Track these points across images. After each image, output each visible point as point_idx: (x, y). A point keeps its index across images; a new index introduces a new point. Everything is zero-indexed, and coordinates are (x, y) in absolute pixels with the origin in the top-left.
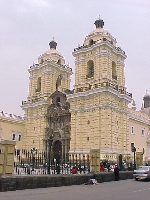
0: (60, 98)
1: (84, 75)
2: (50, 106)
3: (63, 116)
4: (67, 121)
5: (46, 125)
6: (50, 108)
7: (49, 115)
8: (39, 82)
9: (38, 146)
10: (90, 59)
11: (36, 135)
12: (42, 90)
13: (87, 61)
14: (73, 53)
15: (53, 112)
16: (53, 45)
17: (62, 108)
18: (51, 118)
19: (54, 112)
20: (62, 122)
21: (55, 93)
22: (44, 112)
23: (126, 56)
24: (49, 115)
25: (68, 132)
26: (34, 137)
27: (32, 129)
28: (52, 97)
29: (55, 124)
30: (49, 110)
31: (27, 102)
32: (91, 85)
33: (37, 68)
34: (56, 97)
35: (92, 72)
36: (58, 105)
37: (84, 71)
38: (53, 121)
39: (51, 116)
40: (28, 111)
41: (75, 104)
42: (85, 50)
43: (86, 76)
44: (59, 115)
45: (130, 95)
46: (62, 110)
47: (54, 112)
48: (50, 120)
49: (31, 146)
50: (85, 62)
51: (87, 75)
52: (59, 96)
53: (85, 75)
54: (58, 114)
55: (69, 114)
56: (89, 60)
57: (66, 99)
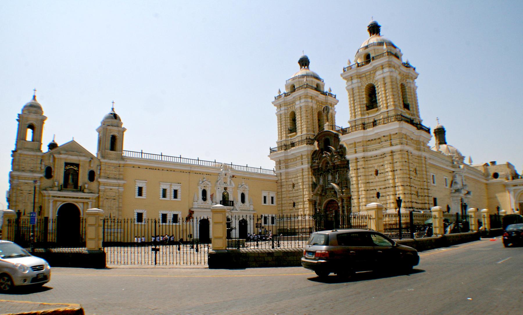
1: (362, 106)
2: (315, 152)
4: (344, 172)
5: (311, 179)
6: (315, 155)
8: (291, 119)
10: (369, 83)
11: (297, 194)
12: (299, 131)
13: (366, 85)
14: (342, 75)
16: (304, 62)
18: (318, 169)
20: (335, 174)
21: (318, 134)
23: (418, 74)
25: (347, 187)
27: (290, 186)
28: (317, 138)
29: (325, 176)
31: (276, 149)
32: (376, 119)
34: (323, 138)
35: (374, 100)
36: (329, 150)
37: (362, 100)
39: (318, 166)
40: (282, 162)
43: (367, 107)
44: (331, 165)
45: (427, 130)
48: (316, 171)
49: (291, 210)
50: (362, 87)
51: (367, 105)
52: (328, 137)
53: (365, 106)
54: (330, 162)
56: (367, 84)
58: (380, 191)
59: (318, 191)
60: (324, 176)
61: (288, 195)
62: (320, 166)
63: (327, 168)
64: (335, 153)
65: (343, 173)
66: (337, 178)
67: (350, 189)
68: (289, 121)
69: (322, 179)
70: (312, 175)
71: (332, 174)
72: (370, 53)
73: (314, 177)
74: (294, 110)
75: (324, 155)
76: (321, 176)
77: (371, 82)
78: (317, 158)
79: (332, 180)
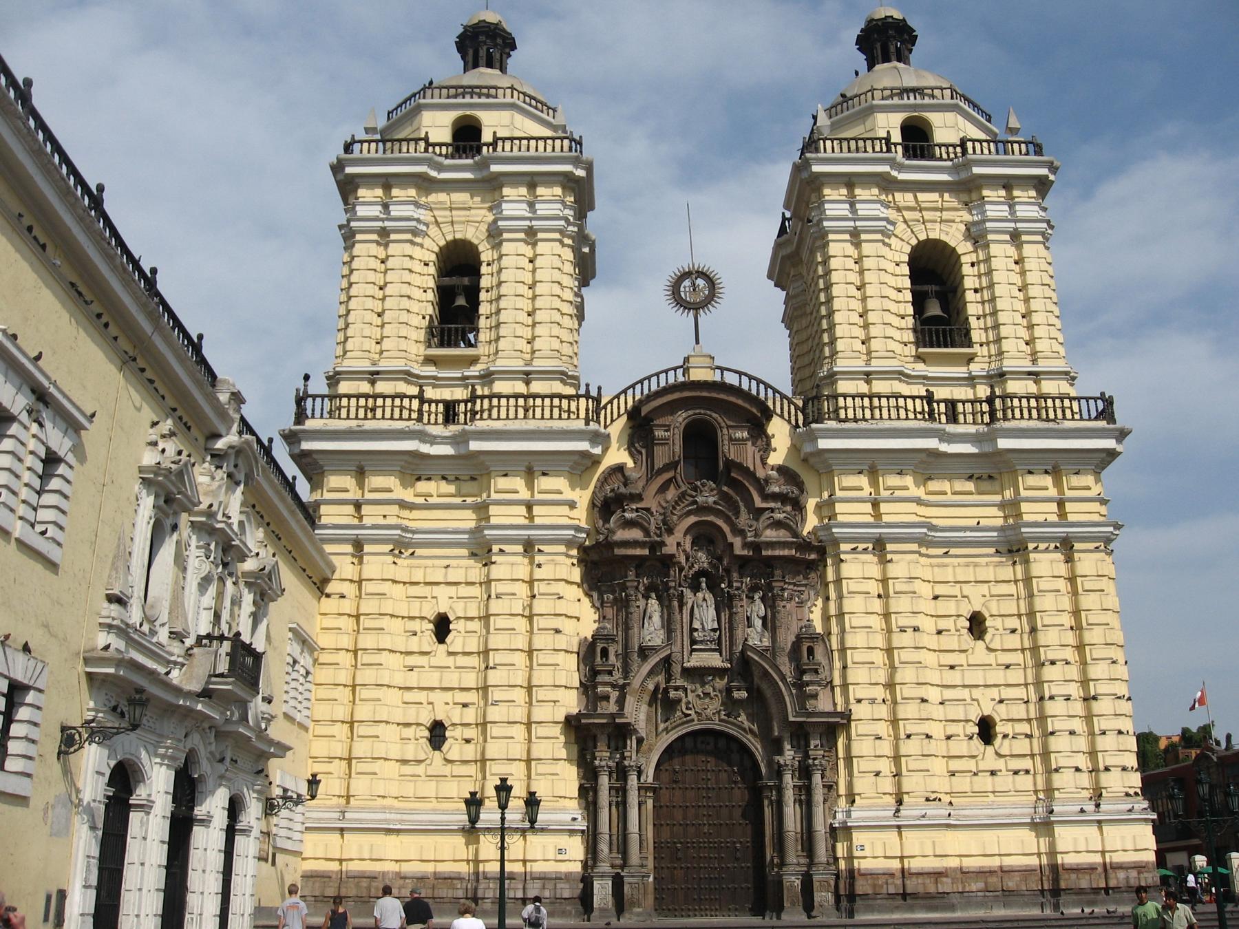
0: (724, 435)
1: (896, 321)
3: (771, 562)
7: (636, 534)
10: (933, 235)
13: (914, 242)
15: (681, 518)
18: (639, 562)
19: (692, 519)
24: (636, 534)
26: (433, 696)
30: (639, 498)
33: (440, 168)
34: (681, 418)
35: (934, 309)
37: (893, 294)
39: (655, 546)
42: (901, 168)
44: (738, 550)
46: (779, 516)
47: (692, 519)
55: (813, 556)
57: (767, 448)
58: (999, 713)
59: (651, 673)
60: (675, 603)
61: (400, 679)
62: (670, 548)
64: (766, 497)
65: (788, 606)
66: (758, 623)
68: (431, 283)
69: (656, 618)
71: (725, 603)
72: (934, 118)
73: (586, 601)
74: (475, 234)
75: (708, 497)
77: (944, 238)
79: (714, 630)
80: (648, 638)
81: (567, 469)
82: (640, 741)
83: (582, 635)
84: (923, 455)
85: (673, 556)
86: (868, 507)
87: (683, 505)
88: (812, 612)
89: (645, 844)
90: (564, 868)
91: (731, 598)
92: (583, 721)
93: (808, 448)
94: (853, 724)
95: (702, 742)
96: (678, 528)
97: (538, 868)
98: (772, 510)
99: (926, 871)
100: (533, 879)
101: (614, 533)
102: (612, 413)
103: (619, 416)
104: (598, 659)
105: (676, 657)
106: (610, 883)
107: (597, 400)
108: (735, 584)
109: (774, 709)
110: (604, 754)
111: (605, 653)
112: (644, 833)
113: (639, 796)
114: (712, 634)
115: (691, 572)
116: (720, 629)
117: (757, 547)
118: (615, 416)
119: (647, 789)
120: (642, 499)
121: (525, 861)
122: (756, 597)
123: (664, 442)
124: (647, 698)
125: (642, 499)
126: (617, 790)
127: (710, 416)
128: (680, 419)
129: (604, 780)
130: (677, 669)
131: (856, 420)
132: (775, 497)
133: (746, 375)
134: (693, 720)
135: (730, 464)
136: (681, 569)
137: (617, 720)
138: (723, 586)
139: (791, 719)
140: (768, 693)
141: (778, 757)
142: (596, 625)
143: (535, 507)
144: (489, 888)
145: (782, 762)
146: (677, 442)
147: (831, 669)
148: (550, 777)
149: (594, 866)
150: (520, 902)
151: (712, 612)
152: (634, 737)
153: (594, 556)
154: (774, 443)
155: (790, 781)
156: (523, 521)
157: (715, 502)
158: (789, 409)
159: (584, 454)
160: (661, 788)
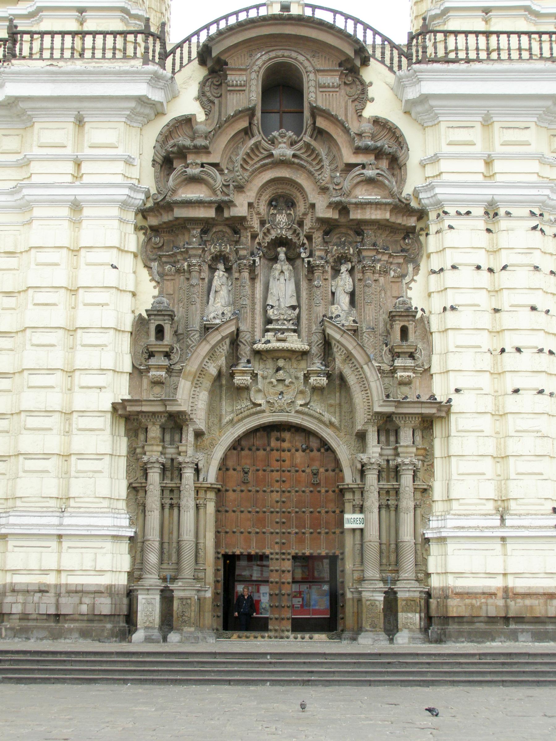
4: (386, 272)
9: (51, 464)
17: (349, 157)
20: (329, 276)
22: (120, 167)
29: (253, 279)
30: (205, 150)
38: (220, 257)
41: (478, 149)
46: (370, 173)
55: (412, 222)
59: (212, 355)
60: (246, 274)
63: (268, 230)
64: (358, 150)
65: (382, 280)
66: (344, 300)
67: (427, 372)
69: (224, 293)
70: (135, 256)
73: (144, 273)
76: (220, 274)
78: (214, 158)
79: (293, 308)
80: (212, 316)
81: (124, 119)
82: (199, 434)
83: (137, 314)
84: (549, 103)
85: (243, 219)
86: (480, 166)
87: (257, 159)
88: (411, 289)
89: (201, 553)
90: (105, 580)
91: (311, 269)
92: (129, 409)
93: (412, 94)
94: (453, 417)
95: (277, 439)
96: (249, 186)
97: (74, 580)
98: (364, 166)
99: (534, 591)
100: (69, 592)
101: (174, 191)
102: (181, 58)
103: (190, 61)
104: (152, 338)
105: (245, 337)
106: (158, 597)
107: (161, 37)
108: (318, 253)
109: (358, 397)
110: (155, 448)
111: (160, 331)
112: (201, 541)
113: (196, 499)
114: (289, 312)
115: (268, 240)
116: (299, 306)
117: (343, 209)
118: (185, 61)
119: (208, 489)
120: (209, 153)
121: (59, 571)
122: (343, 268)
123: (241, 89)
124: (207, 383)
125: (209, 153)
126: (172, 491)
127: (296, 59)
128: (259, 63)
129: (154, 476)
130: (245, 351)
131: (468, 61)
132: (366, 150)
133: (342, 14)
134: (264, 411)
135: (315, 112)
136: (254, 236)
137: (169, 408)
138: (303, 255)
139: (377, 409)
140: (352, 379)
141: (362, 455)
142: (152, 301)
143: (83, 165)
144: (17, 603)
145: (365, 461)
146: (253, 88)
147: (431, 352)
148: (91, 474)
149: (140, 578)
150: (52, 618)
151: (291, 286)
152: (191, 429)
153: (153, 221)
154: (371, 92)
155: (376, 482)
156: (69, 179)
157: (294, 156)
158: (392, 54)
159: (142, 100)
160: (227, 491)
